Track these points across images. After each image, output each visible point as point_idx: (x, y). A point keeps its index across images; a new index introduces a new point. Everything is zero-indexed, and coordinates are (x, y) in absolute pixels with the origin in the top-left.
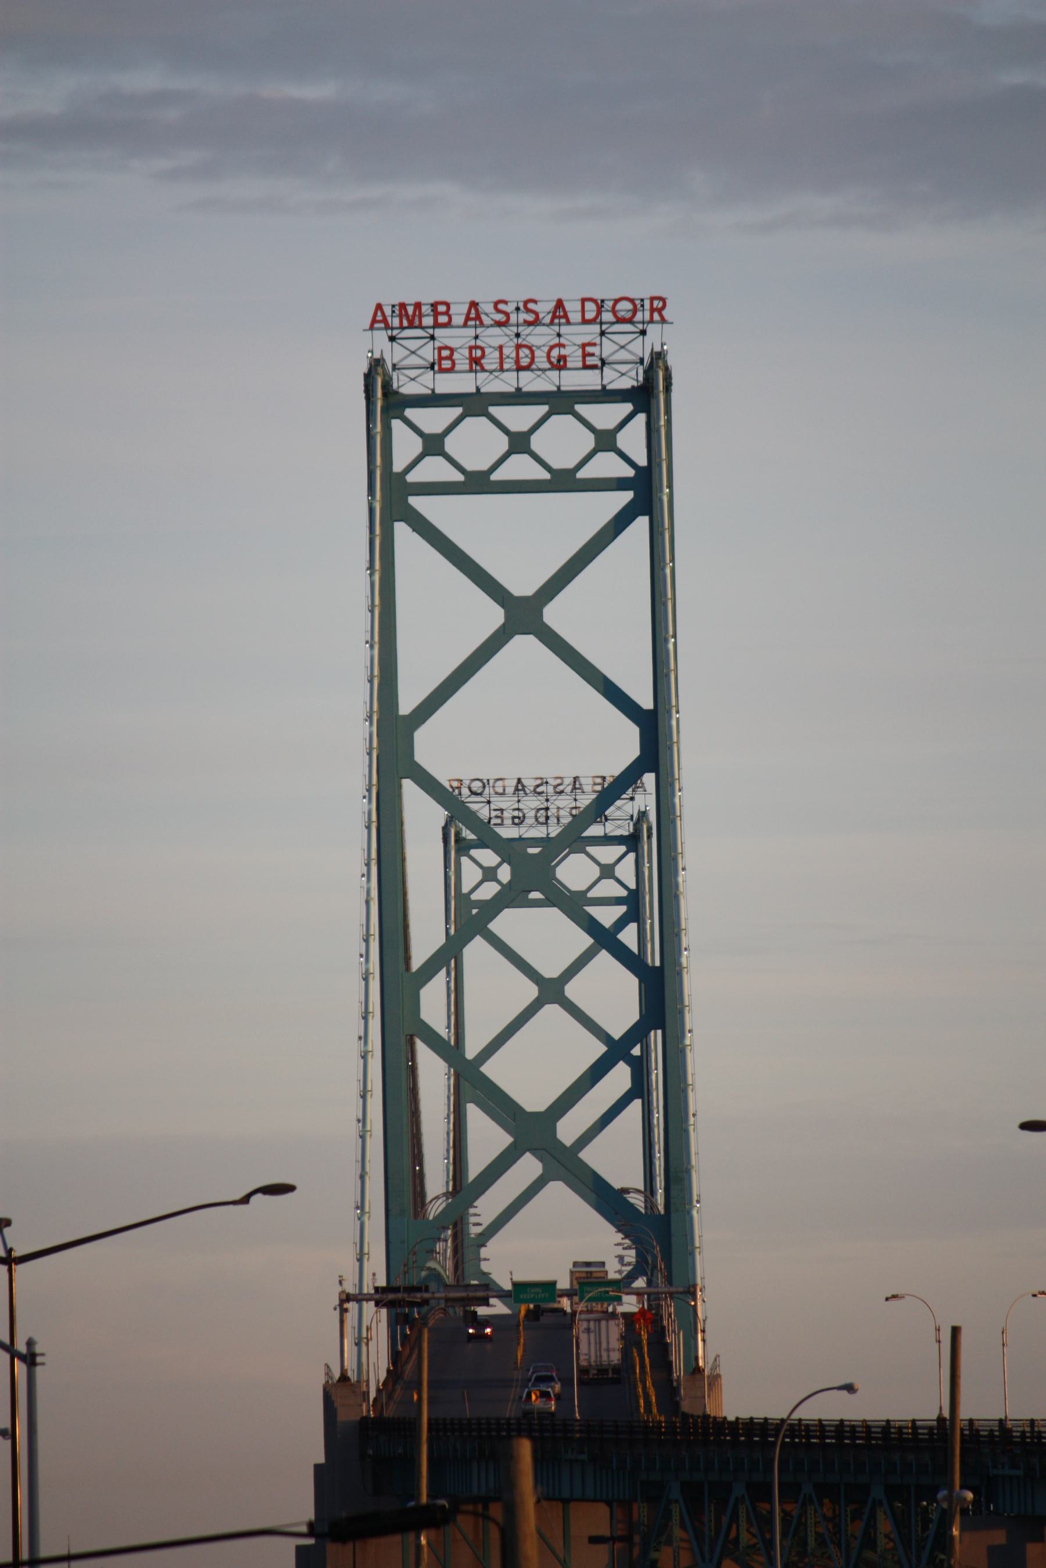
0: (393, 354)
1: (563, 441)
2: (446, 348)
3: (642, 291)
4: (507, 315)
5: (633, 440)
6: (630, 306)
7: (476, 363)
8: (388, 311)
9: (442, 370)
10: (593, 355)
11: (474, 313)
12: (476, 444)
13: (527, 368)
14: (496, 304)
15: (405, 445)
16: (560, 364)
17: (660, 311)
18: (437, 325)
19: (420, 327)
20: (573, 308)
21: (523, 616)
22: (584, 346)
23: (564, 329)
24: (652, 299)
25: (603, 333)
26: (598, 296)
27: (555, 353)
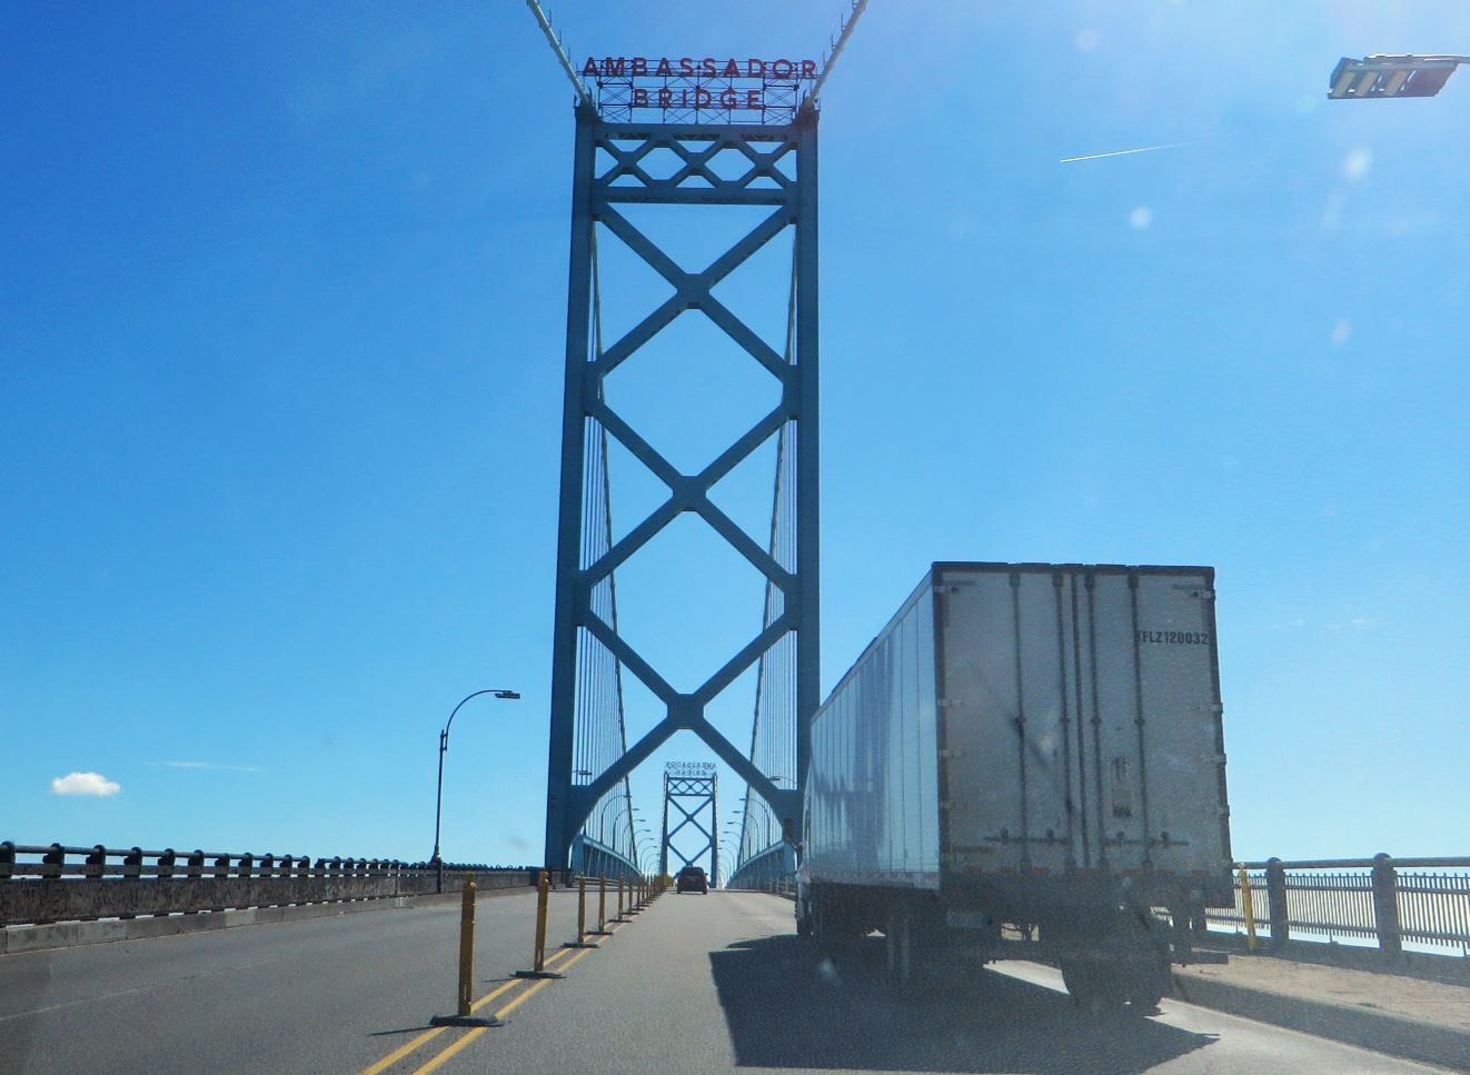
0: (604, 96)
1: (730, 165)
2: (641, 91)
3: (797, 56)
4: (691, 70)
5: (787, 165)
6: (787, 68)
7: (664, 103)
8: (598, 65)
9: (637, 105)
10: (756, 100)
11: (664, 70)
12: (661, 164)
13: (705, 106)
14: (682, 62)
15: (604, 162)
16: (732, 106)
17: (810, 71)
18: (635, 74)
19: (622, 75)
20: (742, 67)
21: (693, 292)
22: (750, 93)
23: (737, 83)
24: (805, 62)
25: (765, 86)
26: (764, 61)
27: (726, 98)
